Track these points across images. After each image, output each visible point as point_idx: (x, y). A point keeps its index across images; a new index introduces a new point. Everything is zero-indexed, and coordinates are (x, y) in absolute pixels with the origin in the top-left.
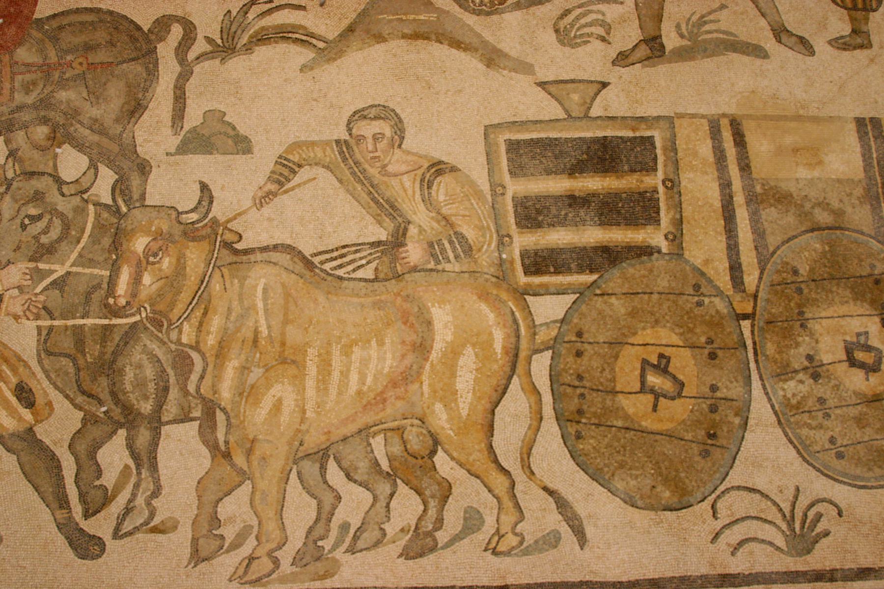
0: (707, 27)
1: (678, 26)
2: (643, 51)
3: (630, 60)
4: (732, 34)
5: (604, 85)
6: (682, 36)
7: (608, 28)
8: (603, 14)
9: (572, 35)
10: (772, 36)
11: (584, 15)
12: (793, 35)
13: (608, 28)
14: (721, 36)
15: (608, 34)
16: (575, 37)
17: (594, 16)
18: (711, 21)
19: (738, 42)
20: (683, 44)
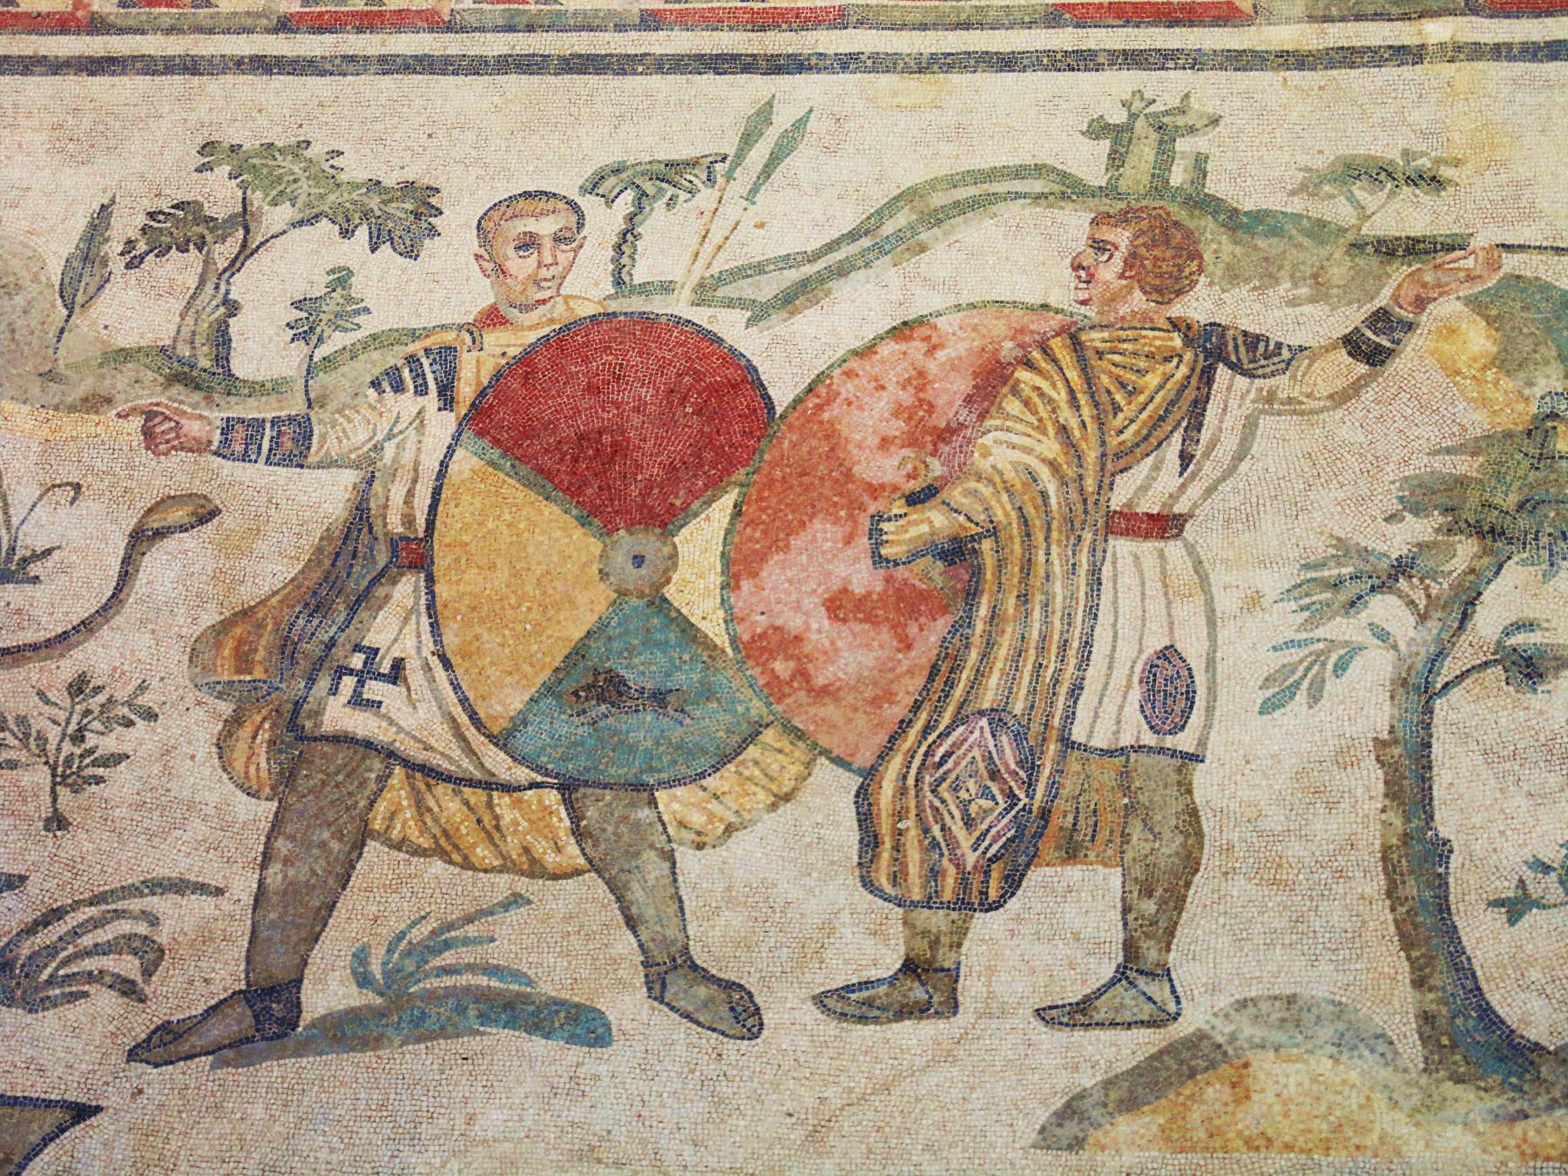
0: (448, 958)
1: (361, 957)
2: (239, 1020)
3: (185, 1048)
4: (517, 975)
5: (82, 1112)
6: (363, 980)
7: (151, 954)
8: (153, 921)
9: (44, 976)
10: (639, 980)
11: (97, 923)
12: (708, 978)
13: (151, 954)
14: (483, 981)
15: (148, 973)
16: (50, 982)
17: (125, 926)
18: (477, 941)
19: (524, 998)
20: (356, 1001)
